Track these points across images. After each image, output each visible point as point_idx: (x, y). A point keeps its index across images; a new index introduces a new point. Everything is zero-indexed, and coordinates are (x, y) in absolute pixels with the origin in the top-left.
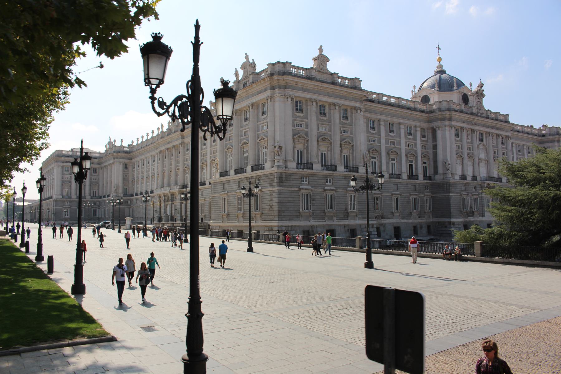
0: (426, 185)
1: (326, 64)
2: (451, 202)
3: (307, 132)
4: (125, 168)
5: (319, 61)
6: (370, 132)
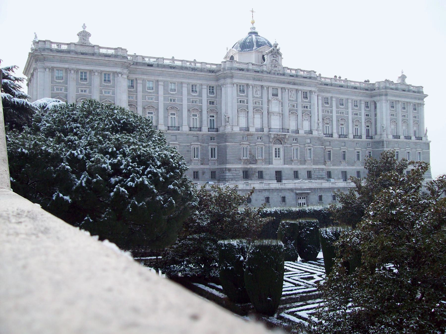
0: (211, 136)
1: (88, 38)
2: (227, 150)
3: (67, 94)
5: (81, 36)
6: (147, 91)
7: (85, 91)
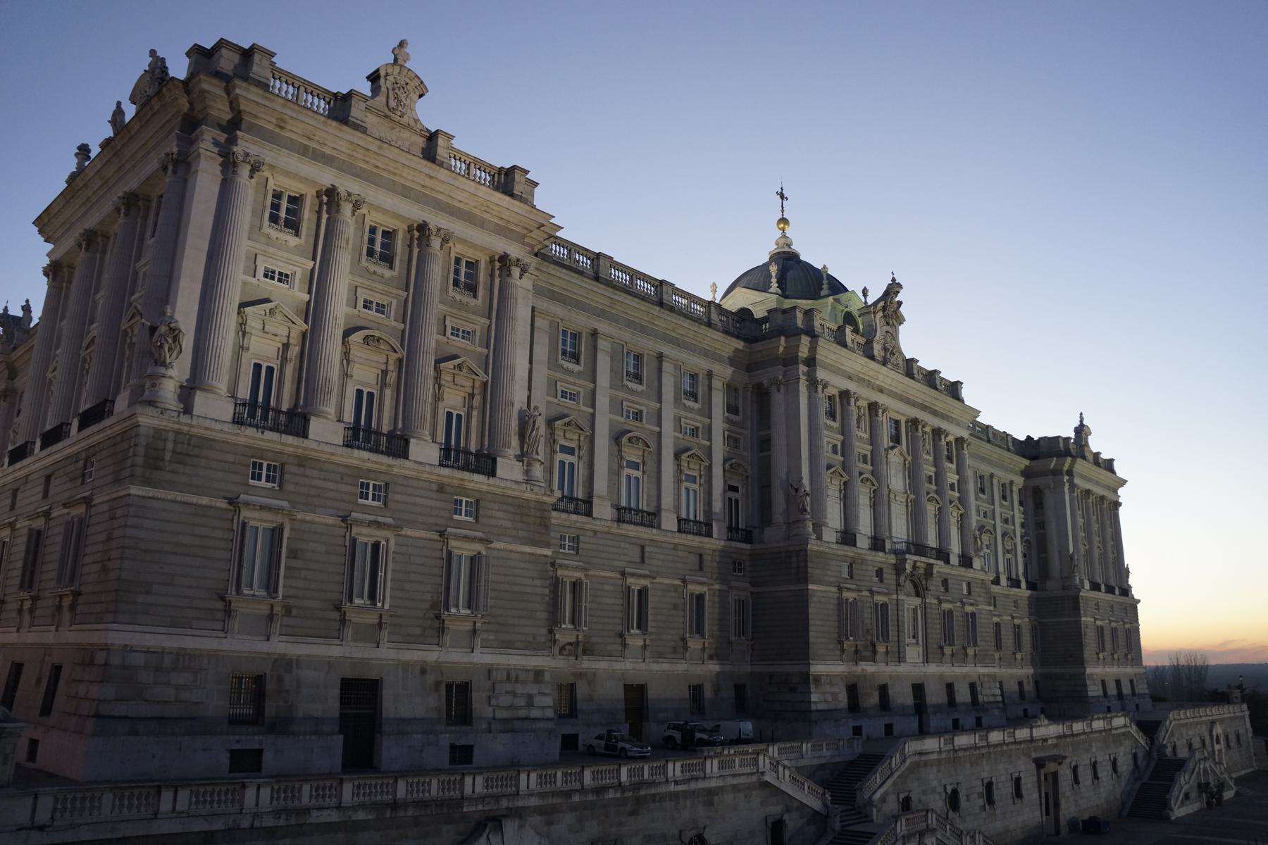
2: (810, 611)
6: (562, 365)
7: (381, 308)
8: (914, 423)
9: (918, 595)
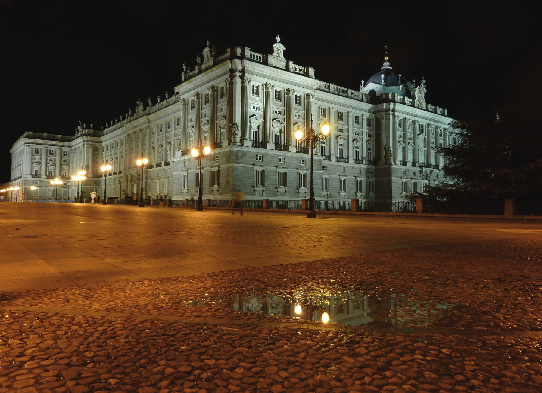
4: (95, 150)
7: (279, 113)
8: (428, 125)
9: (427, 179)
